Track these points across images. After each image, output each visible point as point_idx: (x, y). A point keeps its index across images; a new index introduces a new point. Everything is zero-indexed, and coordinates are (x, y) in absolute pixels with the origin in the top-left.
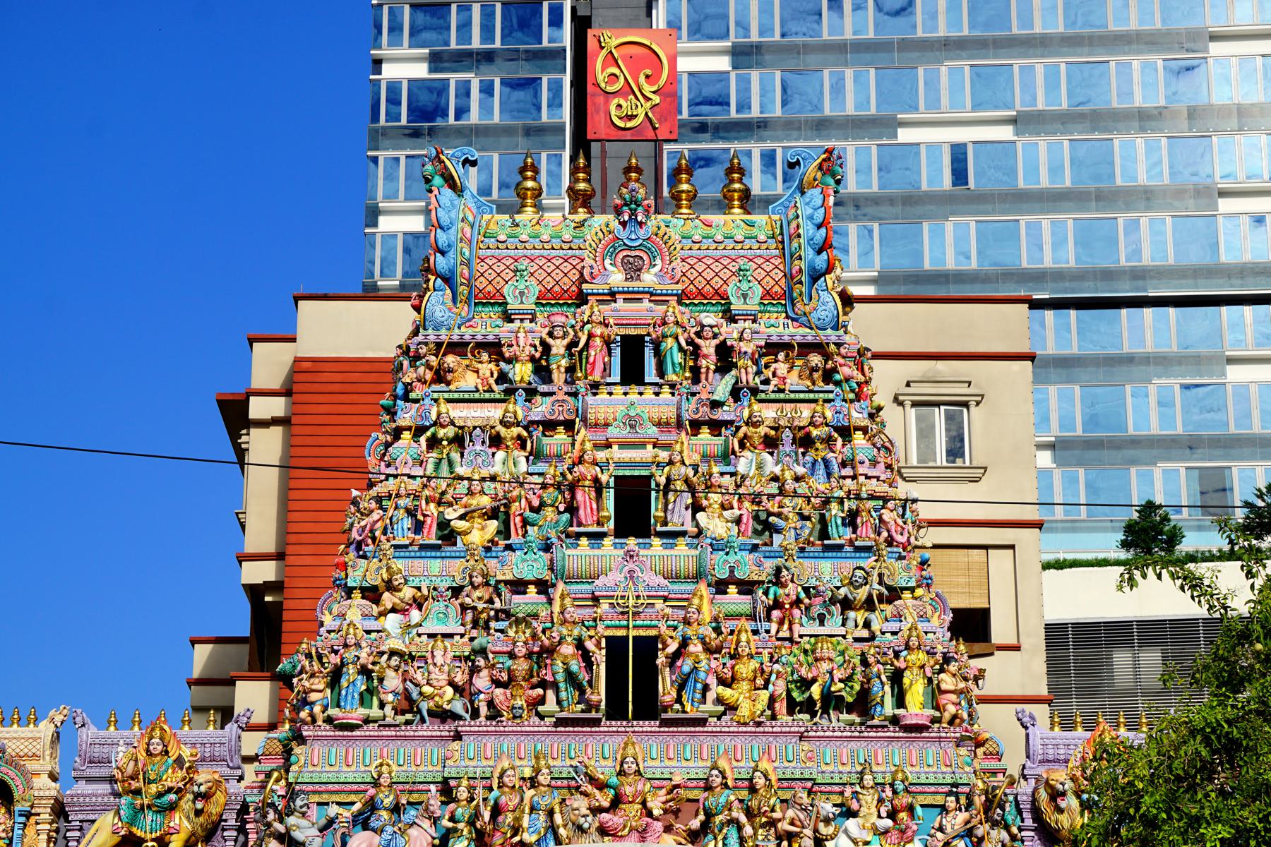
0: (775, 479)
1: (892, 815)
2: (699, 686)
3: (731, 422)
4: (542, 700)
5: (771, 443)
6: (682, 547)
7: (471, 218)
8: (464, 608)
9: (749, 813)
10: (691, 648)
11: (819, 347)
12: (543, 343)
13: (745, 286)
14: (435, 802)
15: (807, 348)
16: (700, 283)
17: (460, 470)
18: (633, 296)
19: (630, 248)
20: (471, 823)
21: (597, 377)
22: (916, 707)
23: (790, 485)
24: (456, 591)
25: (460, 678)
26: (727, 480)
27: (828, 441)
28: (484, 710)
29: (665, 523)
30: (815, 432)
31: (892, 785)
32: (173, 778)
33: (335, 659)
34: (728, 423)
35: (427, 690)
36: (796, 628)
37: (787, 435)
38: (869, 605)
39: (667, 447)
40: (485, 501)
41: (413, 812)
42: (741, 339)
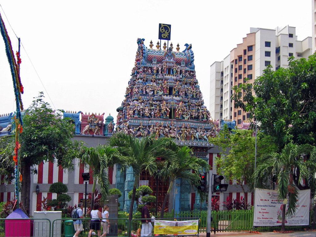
5: (186, 84)
14: (148, 128)
15: (191, 71)
23: (189, 90)
25: (150, 113)
27: (193, 84)
30: (192, 83)
40: (151, 89)
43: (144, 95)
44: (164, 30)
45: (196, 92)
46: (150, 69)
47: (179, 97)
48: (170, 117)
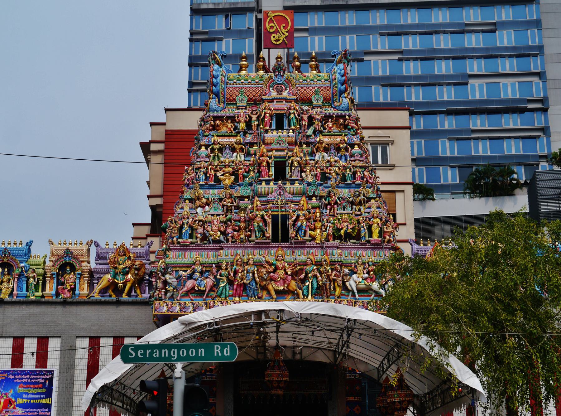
0: (328, 161)
1: (368, 273)
2: (303, 231)
3: (313, 142)
4: (250, 236)
5: (326, 150)
6: (297, 184)
7: (224, 74)
8: (223, 206)
9: (321, 273)
10: (300, 218)
11: (343, 117)
12: (249, 116)
13: (317, 97)
14: (215, 271)
15: (339, 117)
16: (302, 96)
17: (221, 159)
18: (279, 100)
19: (278, 84)
20: (227, 277)
21: (268, 128)
22: (375, 237)
23: (333, 164)
24: (221, 200)
26: (312, 162)
27: (346, 149)
28: (230, 239)
29: (291, 176)
31: (368, 263)
32: (128, 263)
33: (180, 222)
34: (312, 143)
35: (211, 232)
36: (336, 211)
37: (332, 147)
38: (360, 203)
39: (291, 151)
40: (230, 169)
41: (207, 273)
42: (316, 114)
43: (212, 187)
44: (275, 25)
45: (350, 169)
46: (230, 121)
47: (291, 184)
48: (275, 238)
